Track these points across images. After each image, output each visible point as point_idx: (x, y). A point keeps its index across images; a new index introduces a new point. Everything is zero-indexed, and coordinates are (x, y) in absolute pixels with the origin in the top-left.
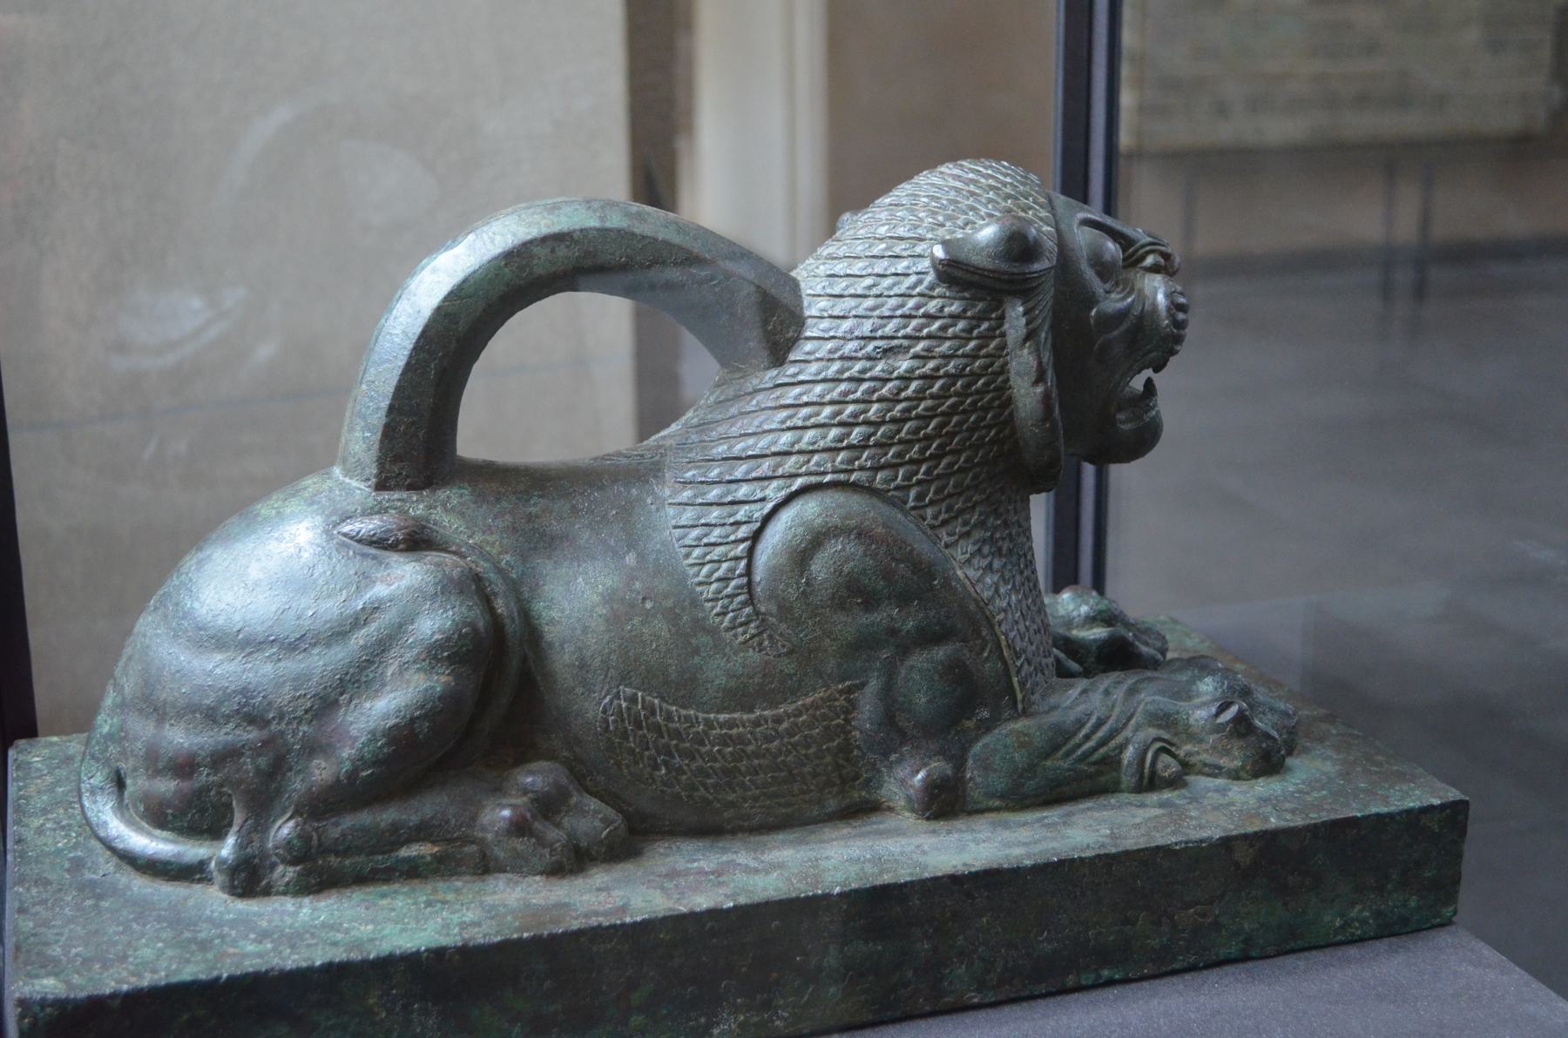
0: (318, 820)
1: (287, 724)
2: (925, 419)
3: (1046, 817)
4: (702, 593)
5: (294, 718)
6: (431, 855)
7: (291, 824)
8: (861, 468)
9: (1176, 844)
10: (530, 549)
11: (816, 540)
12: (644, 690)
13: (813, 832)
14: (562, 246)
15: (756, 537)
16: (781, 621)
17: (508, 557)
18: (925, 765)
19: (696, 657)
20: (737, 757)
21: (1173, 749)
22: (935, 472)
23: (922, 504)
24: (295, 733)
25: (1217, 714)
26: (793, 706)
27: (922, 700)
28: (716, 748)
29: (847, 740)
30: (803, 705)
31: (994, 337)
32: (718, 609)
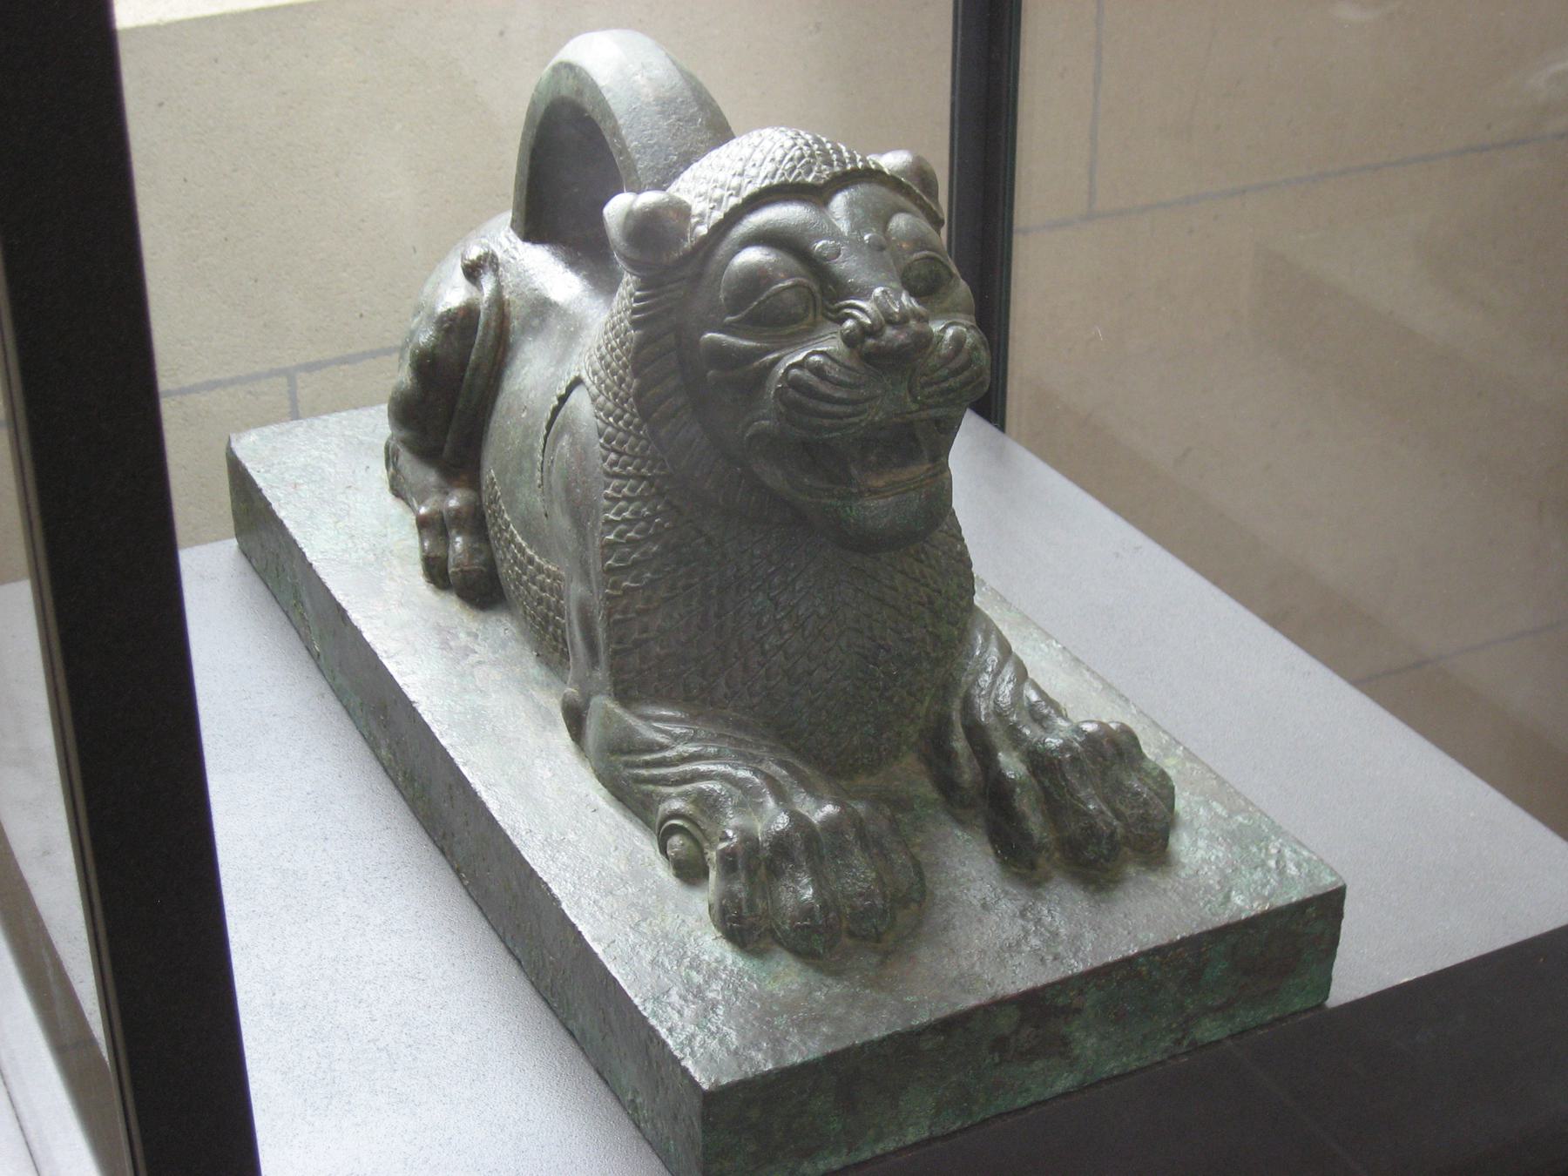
21: (706, 844)
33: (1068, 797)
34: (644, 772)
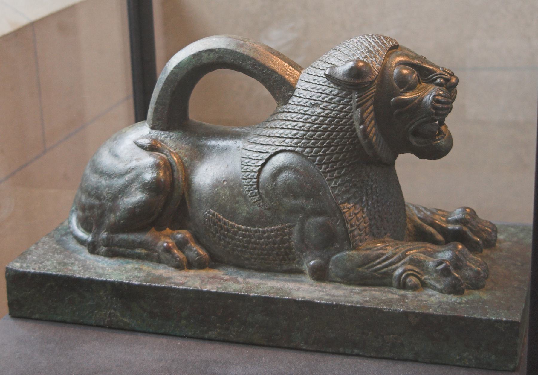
0: (113, 234)
2: (324, 132)
3: (355, 289)
4: (243, 182)
6: (145, 253)
7: (106, 233)
8: (300, 147)
9: (385, 309)
10: (195, 157)
11: (280, 170)
12: (218, 212)
13: (275, 275)
14: (212, 54)
15: (263, 165)
17: (186, 158)
18: (314, 260)
20: (249, 242)
21: (419, 276)
24: (107, 204)
25: (437, 266)
27: (313, 235)
28: (241, 238)
29: (290, 244)
30: (274, 229)
31: (348, 105)
32: (247, 189)
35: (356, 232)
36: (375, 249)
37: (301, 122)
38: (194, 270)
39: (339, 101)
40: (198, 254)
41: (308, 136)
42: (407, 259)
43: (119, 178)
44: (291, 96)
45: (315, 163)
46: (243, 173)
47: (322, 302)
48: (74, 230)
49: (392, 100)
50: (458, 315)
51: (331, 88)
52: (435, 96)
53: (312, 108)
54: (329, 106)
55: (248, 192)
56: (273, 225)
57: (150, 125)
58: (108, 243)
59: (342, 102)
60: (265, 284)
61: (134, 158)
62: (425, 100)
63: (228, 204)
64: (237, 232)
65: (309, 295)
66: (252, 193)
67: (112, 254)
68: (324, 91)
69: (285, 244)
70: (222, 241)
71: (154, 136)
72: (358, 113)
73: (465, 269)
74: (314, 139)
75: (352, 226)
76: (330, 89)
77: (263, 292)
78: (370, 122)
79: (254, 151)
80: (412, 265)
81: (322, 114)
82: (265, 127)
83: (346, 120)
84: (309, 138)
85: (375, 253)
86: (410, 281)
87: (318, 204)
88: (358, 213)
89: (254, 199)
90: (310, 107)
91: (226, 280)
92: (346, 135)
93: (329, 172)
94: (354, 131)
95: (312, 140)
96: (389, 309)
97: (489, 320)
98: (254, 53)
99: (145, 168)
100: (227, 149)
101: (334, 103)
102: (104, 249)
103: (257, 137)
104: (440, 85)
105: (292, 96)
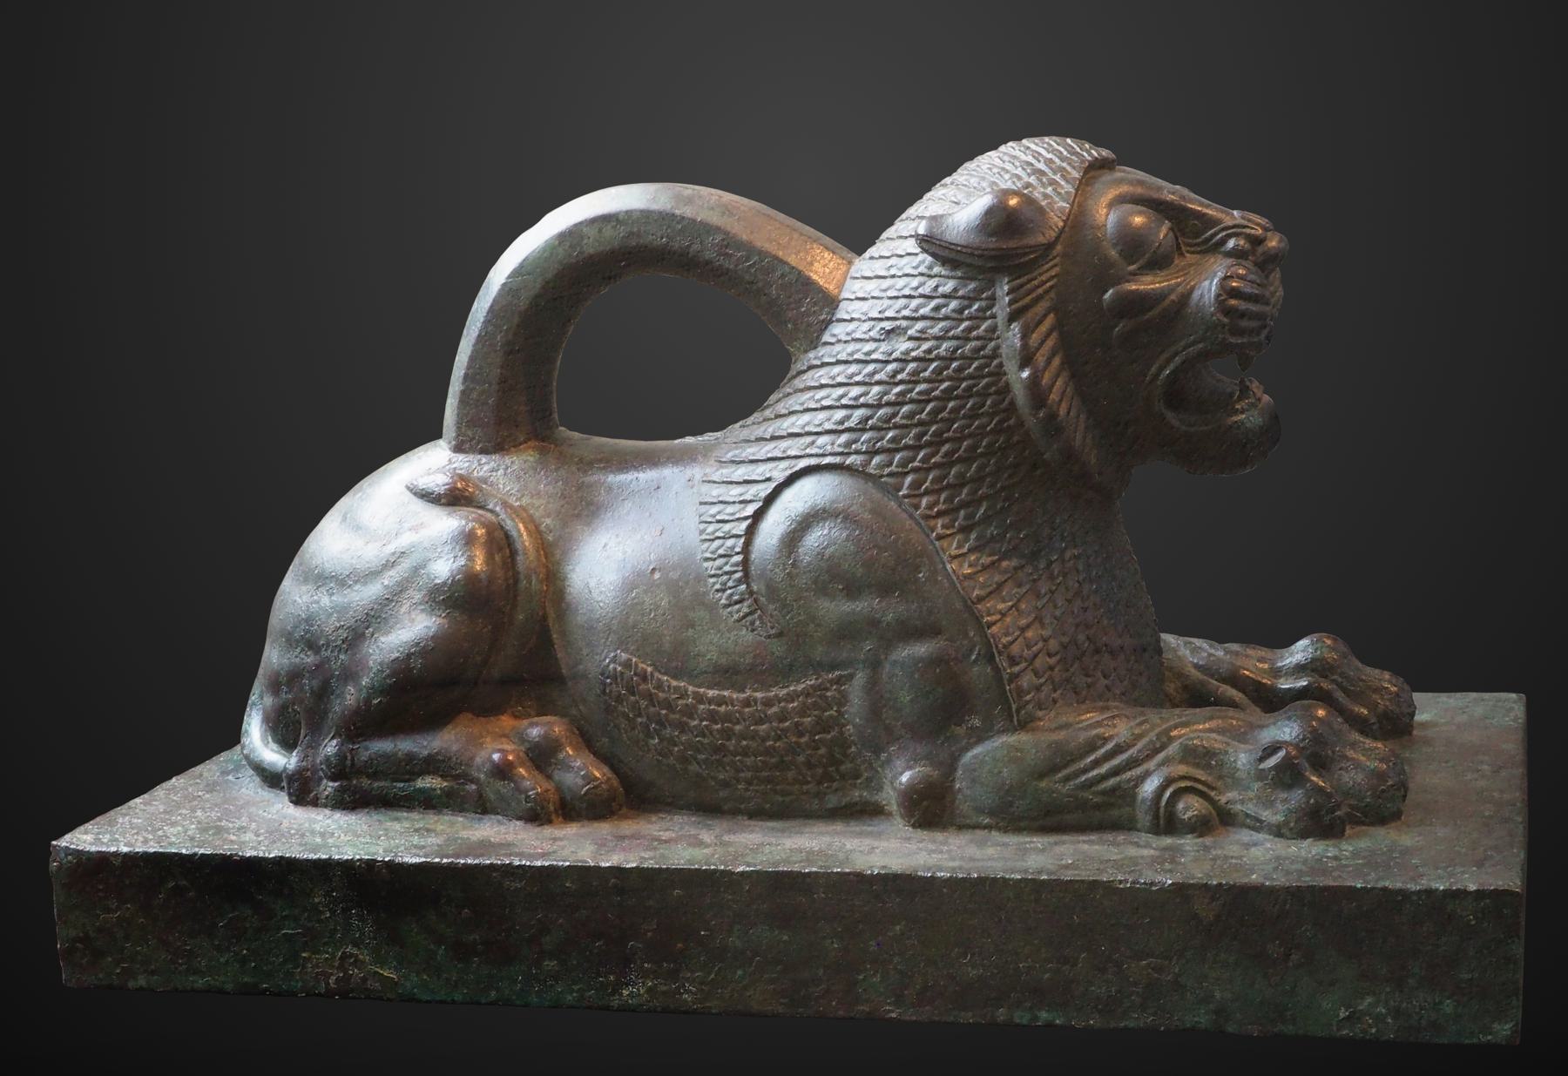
0: (354, 743)
1: (331, 652)
2: (921, 402)
5: (336, 646)
6: (440, 789)
7: (334, 742)
8: (857, 452)
9: (1121, 882)
10: (573, 515)
13: (805, 825)
14: (609, 227)
15: (758, 516)
16: (769, 603)
17: (548, 521)
18: (910, 768)
19: (690, 630)
20: (727, 734)
21: (1213, 794)
22: (933, 461)
23: (916, 492)
24: (337, 658)
25: (1262, 759)
26: (785, 691)
27: (905, 697)
28: (704, 723)
29: (842, 733)
30: (795, 691)
31: (986, 319)
32: (718, 586)
33: (1361, 683)
34: (1095, 772)
35: (1027, 680)
36: (1081, 726)
37: (858, 384)
38: (579, 825)
39: (960, 311)
40: (589, 779)
41: (878, 420)
42: (1173, 749)
43: (365, 584)
44: (827, 323)
45: (901, 493)
46: (706, 545)
47: (939, 874)
48: (253, 750)
49: (1107, 296)
50: (1336, 884)
51: (936, 279)
52: (1226, 278)
53: (886, 342)
54: (932, 327)
55: (720, 594)
56: (792, 681)
57: (450, 442)
58: (341, 770)
59: (966, 312)
60: (779, 844)
61: (406, 525)
62: (1196, 295)
63: (665, 632)
64: (694, 707)
65: (900, 861)
66: (731, 595)
67: (351, 801)
68: (917, 288)
69: (829, 732)
70: (653, 738)
71: (461, 469)
72: (1014, 335)
73: (1340, 769)
74: (896, 427)
75: (1013, 661)
76: (932, 283)
77: (771, 861)
78: (1049, 361)
79: (731, 483)
80: (1187, 763)
81: (914, 354)
82: (761, 419)
83: (982, 361)
84: (881, 424)
85: (1082, 737)
86: (1186, 809)
87: (916, 604)
88: (1028, 626)
89: (739, 611)
90: (879, 340)
91: (666, 842)
92: (984, 405)
93: (940, 514)
94: (1007, 388)
95: (890, 429)
96: (1133, 882)
97: (1429, 892)
98: (722, 216)
99: (434, 547)
100: (658, 488)
101: (946, 318)
102: (329, 787)
103: (741, 447)
104: (1237, 254)
105: (830, 322)
